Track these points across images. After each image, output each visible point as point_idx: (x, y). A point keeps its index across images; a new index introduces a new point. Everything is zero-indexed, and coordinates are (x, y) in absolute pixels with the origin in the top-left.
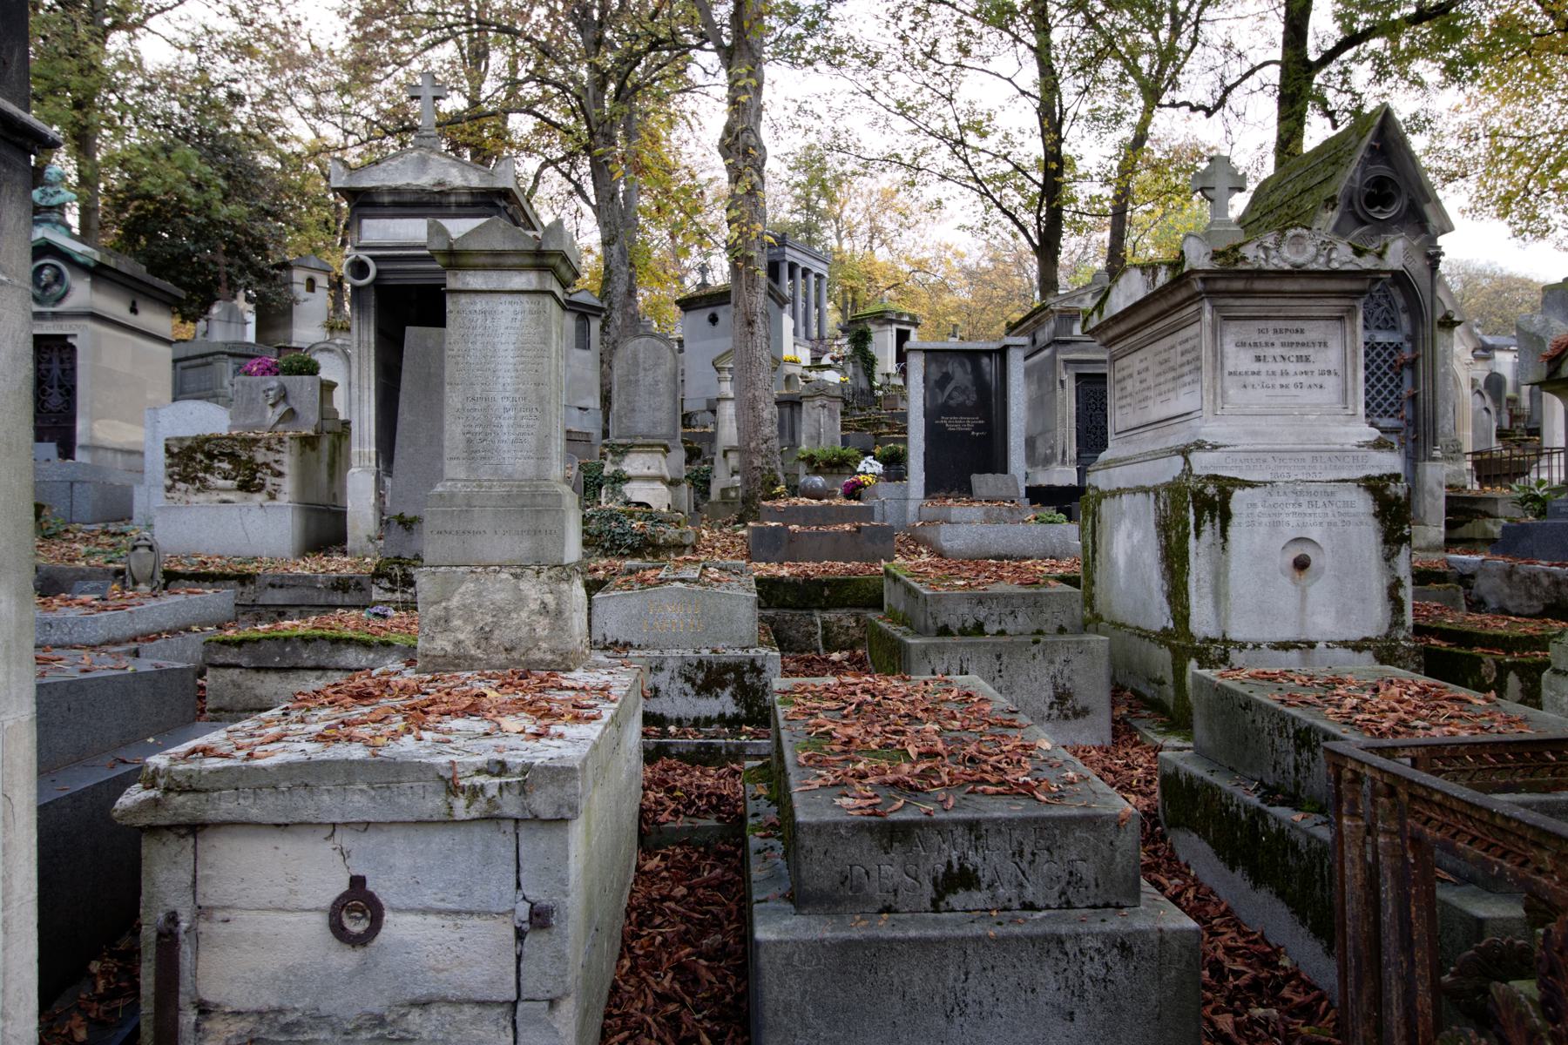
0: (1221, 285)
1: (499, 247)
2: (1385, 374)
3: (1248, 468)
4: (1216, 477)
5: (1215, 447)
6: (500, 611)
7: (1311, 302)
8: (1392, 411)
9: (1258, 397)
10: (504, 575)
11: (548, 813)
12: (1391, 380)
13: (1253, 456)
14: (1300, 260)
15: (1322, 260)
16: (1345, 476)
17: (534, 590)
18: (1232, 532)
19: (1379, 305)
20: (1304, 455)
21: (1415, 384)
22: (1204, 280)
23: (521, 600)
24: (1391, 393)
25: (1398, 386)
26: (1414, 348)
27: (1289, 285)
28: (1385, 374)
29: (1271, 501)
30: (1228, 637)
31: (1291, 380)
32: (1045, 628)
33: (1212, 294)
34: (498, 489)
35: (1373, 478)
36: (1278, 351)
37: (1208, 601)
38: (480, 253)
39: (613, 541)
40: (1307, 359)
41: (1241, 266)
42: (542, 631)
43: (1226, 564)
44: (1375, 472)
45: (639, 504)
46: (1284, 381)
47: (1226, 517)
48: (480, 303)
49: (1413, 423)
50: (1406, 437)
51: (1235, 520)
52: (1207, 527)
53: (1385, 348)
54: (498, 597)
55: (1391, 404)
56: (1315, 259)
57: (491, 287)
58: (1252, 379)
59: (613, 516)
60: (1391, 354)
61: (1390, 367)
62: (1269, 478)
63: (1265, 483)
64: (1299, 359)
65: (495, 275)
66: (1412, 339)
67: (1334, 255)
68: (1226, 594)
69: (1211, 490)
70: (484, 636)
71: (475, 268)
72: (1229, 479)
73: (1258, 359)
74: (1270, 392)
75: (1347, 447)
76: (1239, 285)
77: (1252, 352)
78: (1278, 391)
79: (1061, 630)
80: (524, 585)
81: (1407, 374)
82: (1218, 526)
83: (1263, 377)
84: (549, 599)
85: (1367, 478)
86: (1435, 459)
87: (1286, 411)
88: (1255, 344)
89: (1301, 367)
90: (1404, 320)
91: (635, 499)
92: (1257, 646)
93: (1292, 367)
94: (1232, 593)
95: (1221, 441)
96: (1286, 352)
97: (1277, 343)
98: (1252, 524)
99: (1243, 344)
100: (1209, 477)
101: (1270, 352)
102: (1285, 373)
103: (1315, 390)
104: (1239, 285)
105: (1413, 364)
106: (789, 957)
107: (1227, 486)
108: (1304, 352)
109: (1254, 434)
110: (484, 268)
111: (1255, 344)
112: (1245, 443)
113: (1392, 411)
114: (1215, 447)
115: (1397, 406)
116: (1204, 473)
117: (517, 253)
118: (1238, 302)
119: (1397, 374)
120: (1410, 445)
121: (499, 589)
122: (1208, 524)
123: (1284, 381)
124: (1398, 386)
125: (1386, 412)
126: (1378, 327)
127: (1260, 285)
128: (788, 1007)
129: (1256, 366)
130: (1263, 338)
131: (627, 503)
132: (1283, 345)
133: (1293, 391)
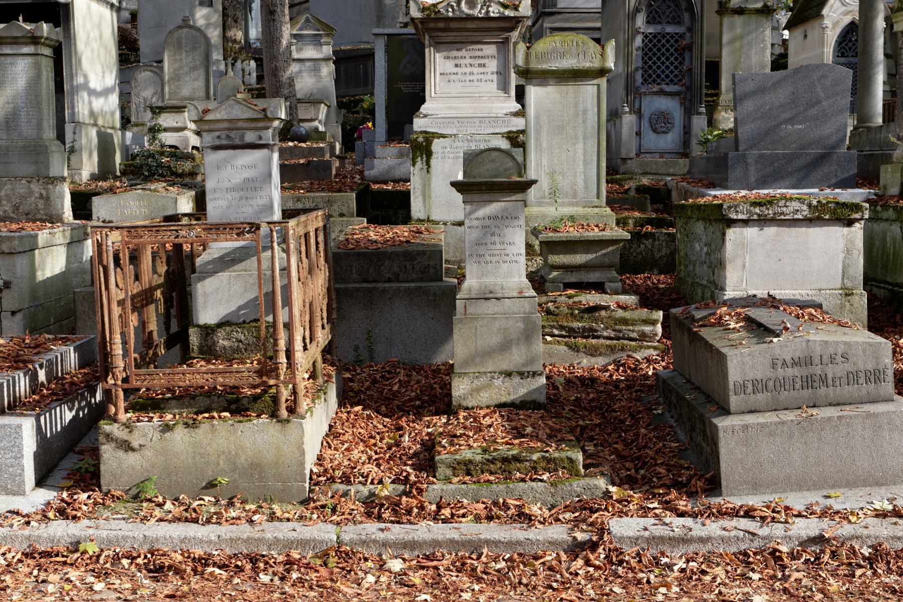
0: (432, 25)
1: (15, 35)
2: (672, 54)
3: (444, 127)
4: (426, 132)
5: (425, 116)
6: (23, 197)
7: (485, 34)
8: (676, 80)
9: (456, 88)
10: (23, 182)
11: (7, 251)
12: (676, 59)
13: (446, 120)
14: (471, 12)
15: (483, 11)
16: (497, 131)
17: (36, 188)
18: (433, 162)
19: (669, 7)
20: (475, 120)
21: (692, 64)
22: (421, 23)
23: (31, 193)
24: (676, 68)
25: (680, 63)
26: (692, 37)
27: (470, 25)
28: (672, 54)
29: (455, 145)
30: (431, 218)
31: (475, 77)
32: (333, 214)
33: (429, 30)
34: (20, 144)
35: (513, 132)
36: (468, 61)
37: (420, 199)
38: (7, 37)
39: (149, 171)
40: (484, 66)
41: (438, 16)
42: (41, 206)
43: (429, 180)
44: (514, 129)
45: (171, 147)
46: (471, 78)
47: (429, 154)
48: (9, 60)
49: (689, 88)
50: (684, 99)
51: (434, 156)
52: (419, 159)
53: (672, 37)
54: (21, 191)
55: (676, 76)
56: (480, 12)
57: (14, 52)
58: (453, 77)
59: (151, 156)
60: (676, 41)
61: (676, 50)
62: (455, 132)
63: (451, 136)
64: (480, 65)
65: (15, 46)
66: (690, 30)
67: (491, 9)
68: (430, 196)
69: (421, 139)
70: (16, 208)
71: (6, 44)
72: (433, 133)
73: (456, 66)
74: (463, 84)
75: (499, 115)
76: (441, 25)
77: (453, 62)
78: (468, 83)
79: (342, 215)
80: (32, 186)
81: (687, 55)
82: (425, 159)
83: (459, 76)
84: (43, 192)
85: (510, 132)
86: (700, 114)
87: (471, 95)
88: (455, 58)
89: (481, 70)
90: (686, 16)
91: (167, 143)
92: (445, 224)
93: (476, 70)
94: (433, 195)
95: (430, 112)
96: (472, 61)
97: (467, 57)
98: (443, 158)
99: (448, 58)
100: (421, 132)
101: (463, 62)
102: (471, 74)
103: (488, 83)
104: (441, 25)
105: (689, 47)
106: (84, 296)
107: (429, 137)
108: (482, 61)
109: (450, 108)
110: (10, 44)
111: (455, 58)
112: (442, 114)
113: (676, 80)
114: (425, 116)
115: (680, 77)
116: (419, 130)
117: (23, 37)
118: (444, 34)
119: (681, 55)
120: (687, 103)
121: (21, 188)
122: (419, 159)
123: (471, 78)
124: (680, 63)
125: (672, 81)
126: (668, 23)
127: (453, 25)
128: (84, 311)
129: (455, 70)
130: (459, 54)
131: (162, 146)
132: (471, 57)
133: (476, 83)
